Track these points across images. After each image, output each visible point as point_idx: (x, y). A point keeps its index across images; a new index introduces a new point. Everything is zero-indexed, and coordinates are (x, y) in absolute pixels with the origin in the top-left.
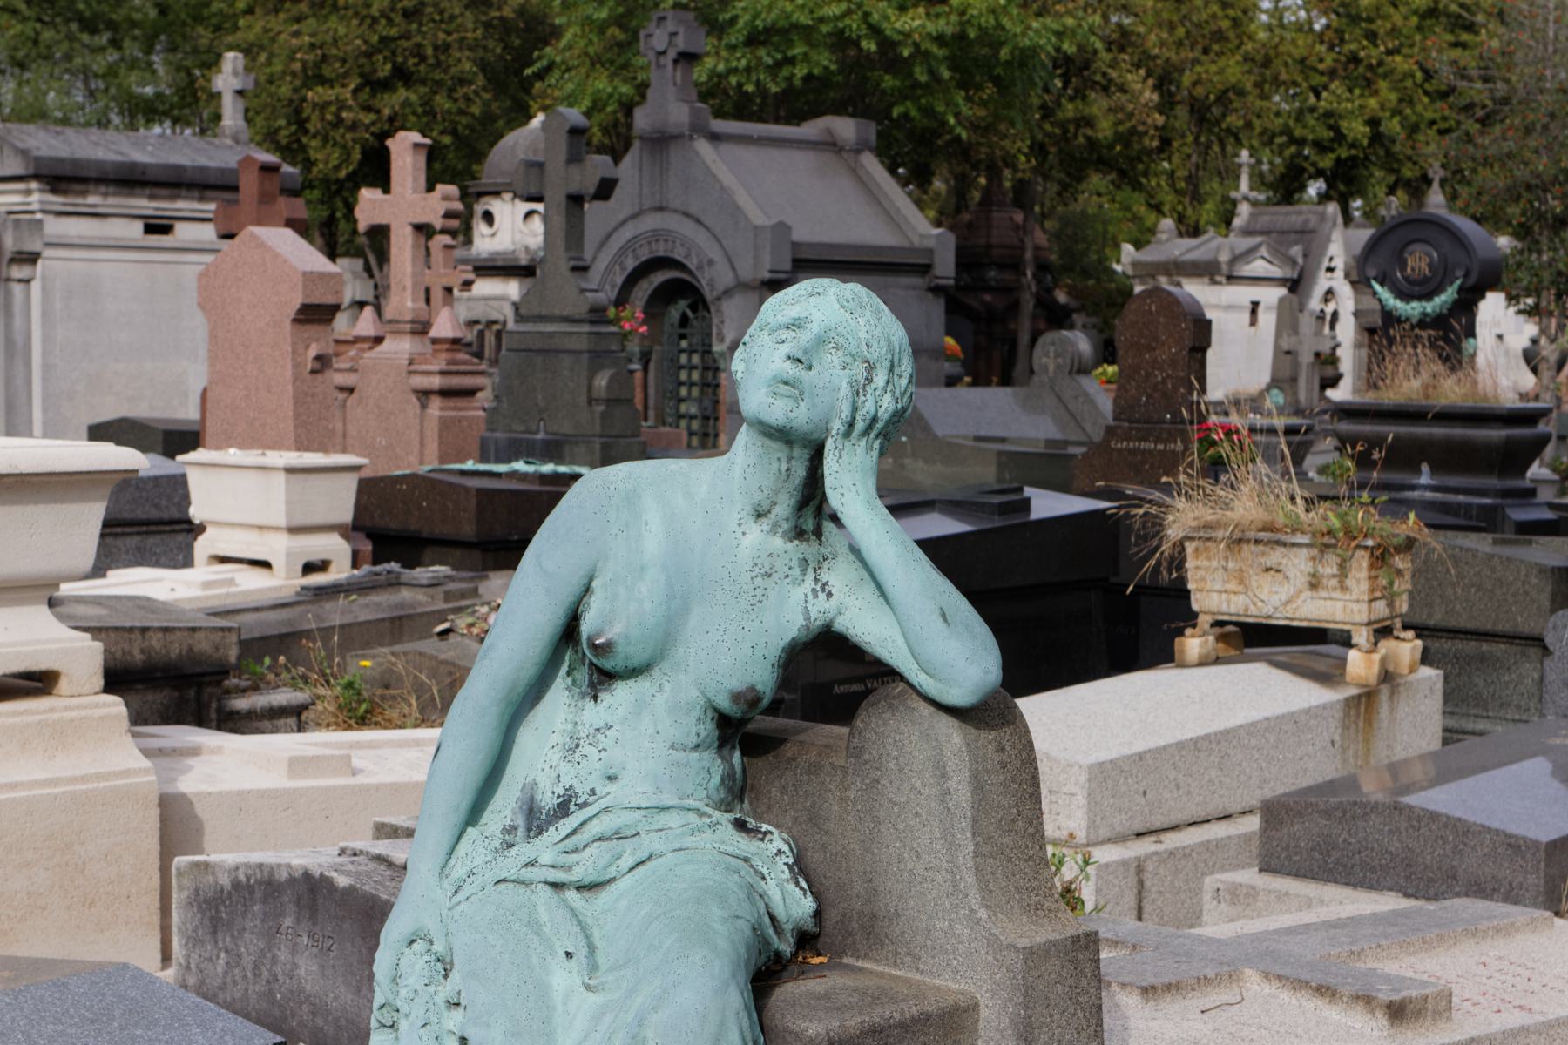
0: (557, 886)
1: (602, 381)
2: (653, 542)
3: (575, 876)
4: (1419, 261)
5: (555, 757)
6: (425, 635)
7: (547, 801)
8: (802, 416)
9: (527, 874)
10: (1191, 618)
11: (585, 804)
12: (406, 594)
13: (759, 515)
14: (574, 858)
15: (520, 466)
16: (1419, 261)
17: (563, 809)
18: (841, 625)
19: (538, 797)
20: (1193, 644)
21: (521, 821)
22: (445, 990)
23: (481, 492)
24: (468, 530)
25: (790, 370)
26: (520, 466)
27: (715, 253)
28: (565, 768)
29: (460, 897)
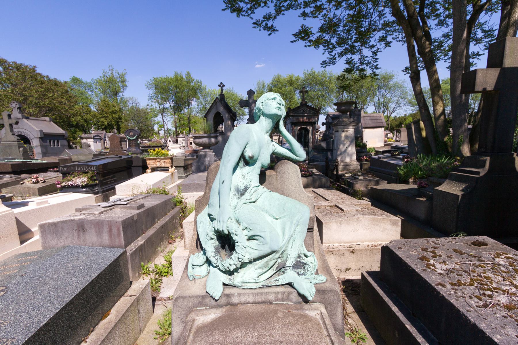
0: (251, 203)
1: (21, 149)
2: (256, 139)
3: (253, 200)
4: (132, 134)
5: (241, 179)
6: (18, 184)
7: (242, 188)
8: (276, 115)
9: (246, 202)
10: (148, 168)
11: (249, 187)
12: (5, 179)
13: (267, 133)
14: (251, 197)
15: (16, 160)
16: (132, 134)
17: (246, 189)
18: (276, 151)
19: (239, 187)
20: (149, 171)
21: (236, 193)
22: (241, 227)
23: (11, 164)
24: (10, 170)
25: (278, 105)
26: (16, 160)
27: (30, 134)
28: (244, 181)
29: (236, 209)
